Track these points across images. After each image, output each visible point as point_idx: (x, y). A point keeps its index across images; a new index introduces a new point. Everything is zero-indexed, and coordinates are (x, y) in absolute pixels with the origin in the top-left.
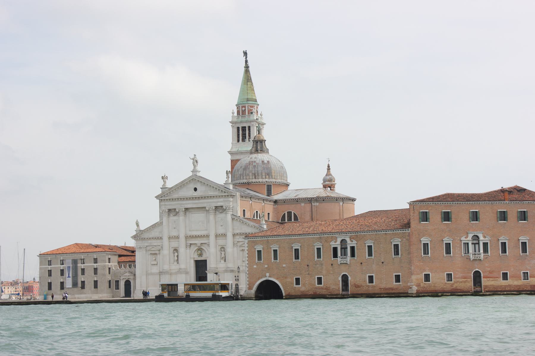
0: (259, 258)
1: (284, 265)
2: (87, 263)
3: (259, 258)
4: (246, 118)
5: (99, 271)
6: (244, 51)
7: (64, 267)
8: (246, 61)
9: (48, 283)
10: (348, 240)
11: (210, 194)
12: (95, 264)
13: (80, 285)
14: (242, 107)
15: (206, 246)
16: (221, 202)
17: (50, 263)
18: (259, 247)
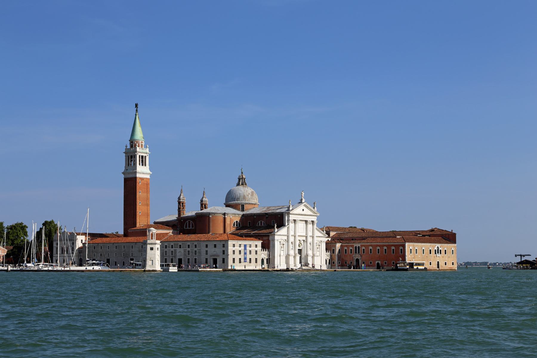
0: (411, 253)
1: (419, 256)
2: (252, 247)
3: (411, 253)
4: (144, 151)
5: (258, 252)
6: (136, 104)
7: (241, 249)
8: (137, 110)
9: (233, 258)
10: (439, 247)
11: (309, 213)
12: (256, 248)
13: (248, 260)
14: (141, 142)
15: (303, 241)
16: (313, 218)
17: (234, 246)
18: (411, 248)
